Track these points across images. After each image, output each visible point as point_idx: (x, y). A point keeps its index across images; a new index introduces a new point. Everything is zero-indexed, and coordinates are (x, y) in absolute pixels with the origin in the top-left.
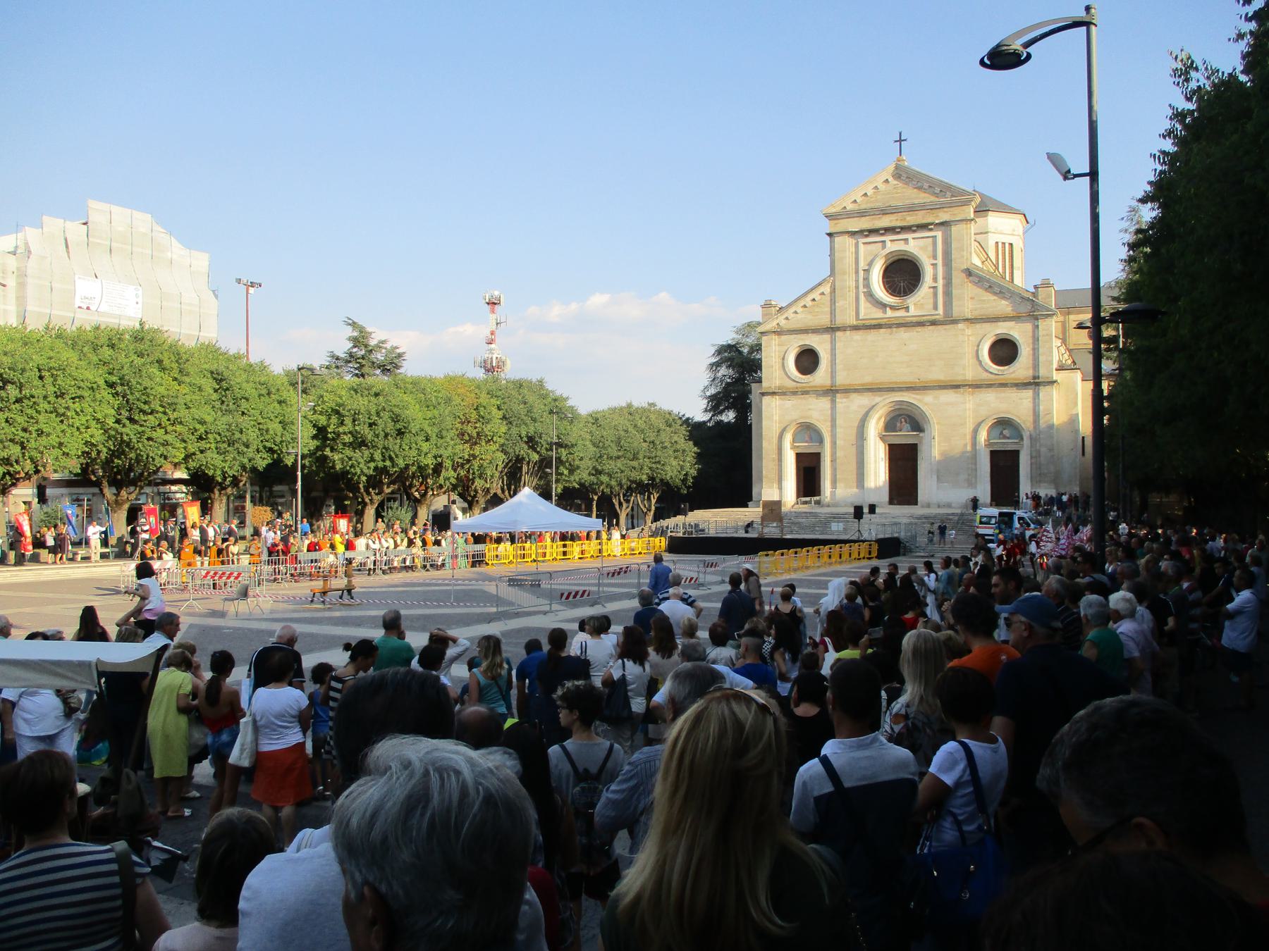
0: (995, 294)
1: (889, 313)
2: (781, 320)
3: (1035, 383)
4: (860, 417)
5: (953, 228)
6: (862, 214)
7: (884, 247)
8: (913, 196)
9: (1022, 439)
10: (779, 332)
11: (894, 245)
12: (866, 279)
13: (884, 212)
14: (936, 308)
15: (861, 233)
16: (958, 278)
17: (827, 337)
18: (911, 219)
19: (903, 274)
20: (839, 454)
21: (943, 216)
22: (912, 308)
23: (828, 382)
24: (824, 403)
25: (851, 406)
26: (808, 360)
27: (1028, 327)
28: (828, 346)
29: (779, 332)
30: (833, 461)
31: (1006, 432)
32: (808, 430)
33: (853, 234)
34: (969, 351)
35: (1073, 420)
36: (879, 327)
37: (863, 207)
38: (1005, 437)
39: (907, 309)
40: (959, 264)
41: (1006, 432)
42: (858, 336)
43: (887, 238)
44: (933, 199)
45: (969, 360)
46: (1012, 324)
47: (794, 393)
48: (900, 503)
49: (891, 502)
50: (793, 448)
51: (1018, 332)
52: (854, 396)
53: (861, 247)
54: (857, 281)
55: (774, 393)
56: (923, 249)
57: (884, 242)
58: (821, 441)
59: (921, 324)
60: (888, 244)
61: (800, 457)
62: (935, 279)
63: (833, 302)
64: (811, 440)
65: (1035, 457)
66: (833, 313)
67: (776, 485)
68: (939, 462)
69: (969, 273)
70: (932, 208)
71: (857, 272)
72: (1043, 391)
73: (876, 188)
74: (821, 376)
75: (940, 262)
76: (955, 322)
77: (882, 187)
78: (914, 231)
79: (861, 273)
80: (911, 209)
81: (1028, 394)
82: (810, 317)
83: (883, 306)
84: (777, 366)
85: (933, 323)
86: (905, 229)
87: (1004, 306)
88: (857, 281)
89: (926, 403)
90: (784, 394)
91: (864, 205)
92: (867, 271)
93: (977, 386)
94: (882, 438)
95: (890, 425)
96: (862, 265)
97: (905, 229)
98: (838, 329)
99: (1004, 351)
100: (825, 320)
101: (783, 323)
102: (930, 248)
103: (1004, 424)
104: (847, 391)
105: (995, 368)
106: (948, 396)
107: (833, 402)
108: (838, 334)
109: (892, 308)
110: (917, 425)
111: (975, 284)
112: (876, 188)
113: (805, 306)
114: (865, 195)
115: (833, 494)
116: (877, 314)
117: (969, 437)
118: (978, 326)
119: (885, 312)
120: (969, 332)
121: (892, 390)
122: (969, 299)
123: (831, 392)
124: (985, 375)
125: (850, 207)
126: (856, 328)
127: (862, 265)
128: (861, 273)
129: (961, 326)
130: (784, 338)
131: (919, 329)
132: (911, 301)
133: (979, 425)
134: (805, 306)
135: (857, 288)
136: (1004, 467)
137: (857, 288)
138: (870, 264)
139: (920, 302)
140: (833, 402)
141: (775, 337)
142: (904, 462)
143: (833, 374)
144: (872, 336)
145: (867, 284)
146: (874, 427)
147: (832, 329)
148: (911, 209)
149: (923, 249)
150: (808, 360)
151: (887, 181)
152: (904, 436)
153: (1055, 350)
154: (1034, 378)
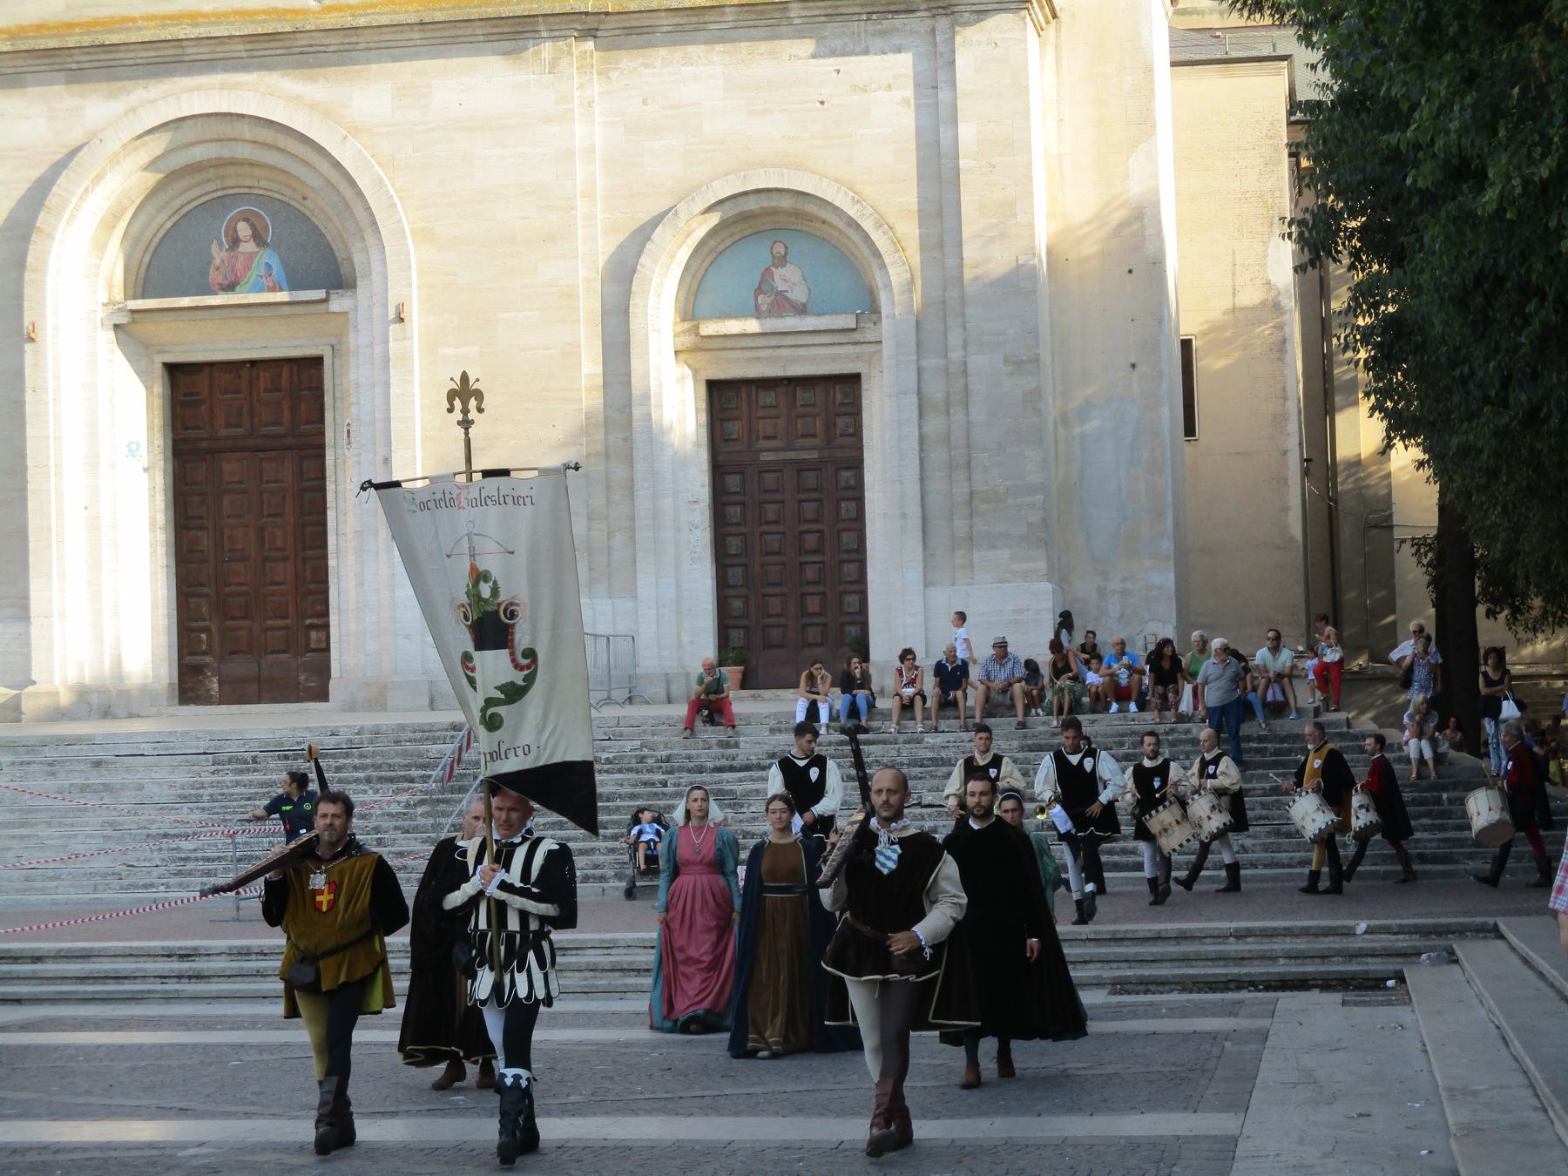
35: (1135, 253)
38: (783, 305)
41: (790, 280)
48: (237, 693)
49: (190, 684)
94: (127, 330)
95: (167, 261)
110: (324, 262)
117: (589, 304)
121: (167, 56)
133: (643, 235)
136: (784, 464)
142: (249, 457)
146: (80, 275)
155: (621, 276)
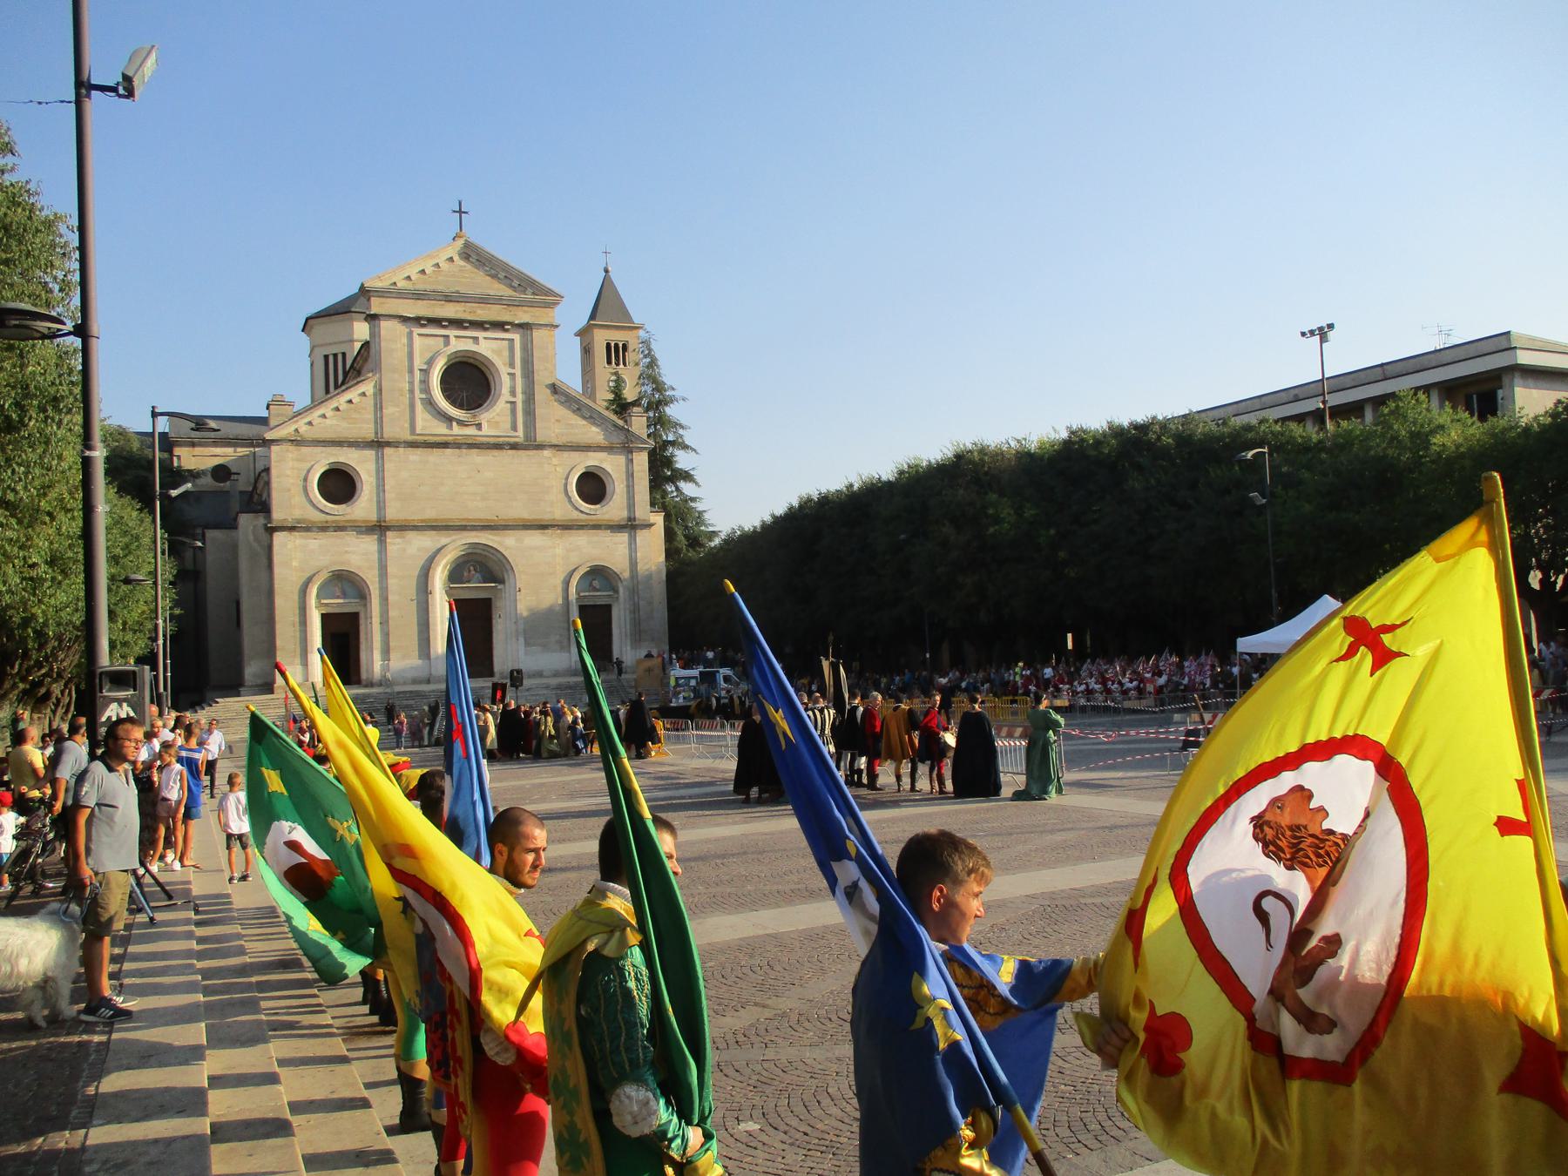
0: (584, 418)
1: (456, 430)
2: (301, 424)
3: (631, 526)
4: (421, 563)
5: (536, 333)
6: (418, 296)
7: (447, 343)
8: (481, 283)
9: (616, 591)
10: (297, 441)
11: (460, 343)
12: (425, 382)
13: (448, 298)
14: (514, 428)
15: (417, 321)
16: (542, 394)
17: (370, 454)
18: (483, 313)
19: (468, 382)
20: (392, 613)
21: (523, 316)
22: (485, 425)
23: (373, 517)
24: (369, 544)
25: (408, 550)
26: (339, 485)
27: (621, 459)
28: (372, 466)
29: (297, 441)
30: (385, 622)
31: (596, 583)
32: (344, 581)
33: (405, 320)
34: (557, 486)
36: (444, 445)
37: (421, 287)
38: (595, 590)
39: (479, 426)
40: (542, 378)
41: (596, 583)
42: (415, 455)
43: (452, 333)
44: (510, 292)
45: (556, 495)
46: (603, 455)
47: (323, 528)
50: (320, 605)
51: (612, 465)
52: (411, 535)
53: (416, 339)
54: (411, 383)
55: (292, 529)
56: (498, 352)
57: (447, 337)
58: (362, 595)
59: (498, 447)
60: (453, 340)
61: (326, 619)
62: (513, 393)
63: (379, 407)
64: (344, 595)
65: (635, 610)
66: (379, 422)
67: (298, 660)
68: (526, 620)
69: (554, 389)
70: (511, 304)
71: (411, 371)
72: (642, 536)
73: (437, 265)
74: (362, 507)
75: (518, 371)
76: (541, 447)
77: (444, 266)
78: (486, 329)
79: (417, 374)
80: (484, 300)
81: (624, 537)
82: (344, 424)
83: (450, 420)
84: (297, 490)
85: (514, 447)
86: (479, 325)
87: (595, 434)
88: (411, 383)
89: (506, 544)
90: (308, 529)
91: (421, 285)
92: (426, 372)
93: (567, 527)
95: (455, 575)
96: (419, 363)
97: (479, 325)
98: (388, 444)
99: (593, 487)
100: (368, 432)
101: (304, 429)
102: (506, 353)
103: (599, 574)
104: (403, 527)
106: (534, 539)
107: (382, 542)
108: (388, 451)
109: (461, 423)
111: (562, 403)
112: (437, 265)
113: (337, 409)
114: (423, 272)
115: (386, 668)
116: (440, 429)
117: (560, 589)
118: (566, 454)
119: (451, 428)
120: (555, 461)
121: (463, 528)
122: (555, 422)
123: (380, 528)
124: (575, 515)
125: (402, 284)
126: (413, 445)
127: (419, 363)
128: (417, 374)
129: (546, 453)
130: (305, 450)
131: (496, 452)
134: (337, 409)
135: (412, 391)
137: (412, 391)
138: (430, 362)
139: (495, 419)
140: (382, 542)
141: (292, 448)
142: (475, 620)
143: (381, 505)
144: (435, 456)
145: (426, 388)
147: (379, 444)
148: (484, 300)
149: (498, 352)
150: (339, 485)
151: (451, 259)
152: (474, 588)
154: (630, 519)
155: (567, 583)
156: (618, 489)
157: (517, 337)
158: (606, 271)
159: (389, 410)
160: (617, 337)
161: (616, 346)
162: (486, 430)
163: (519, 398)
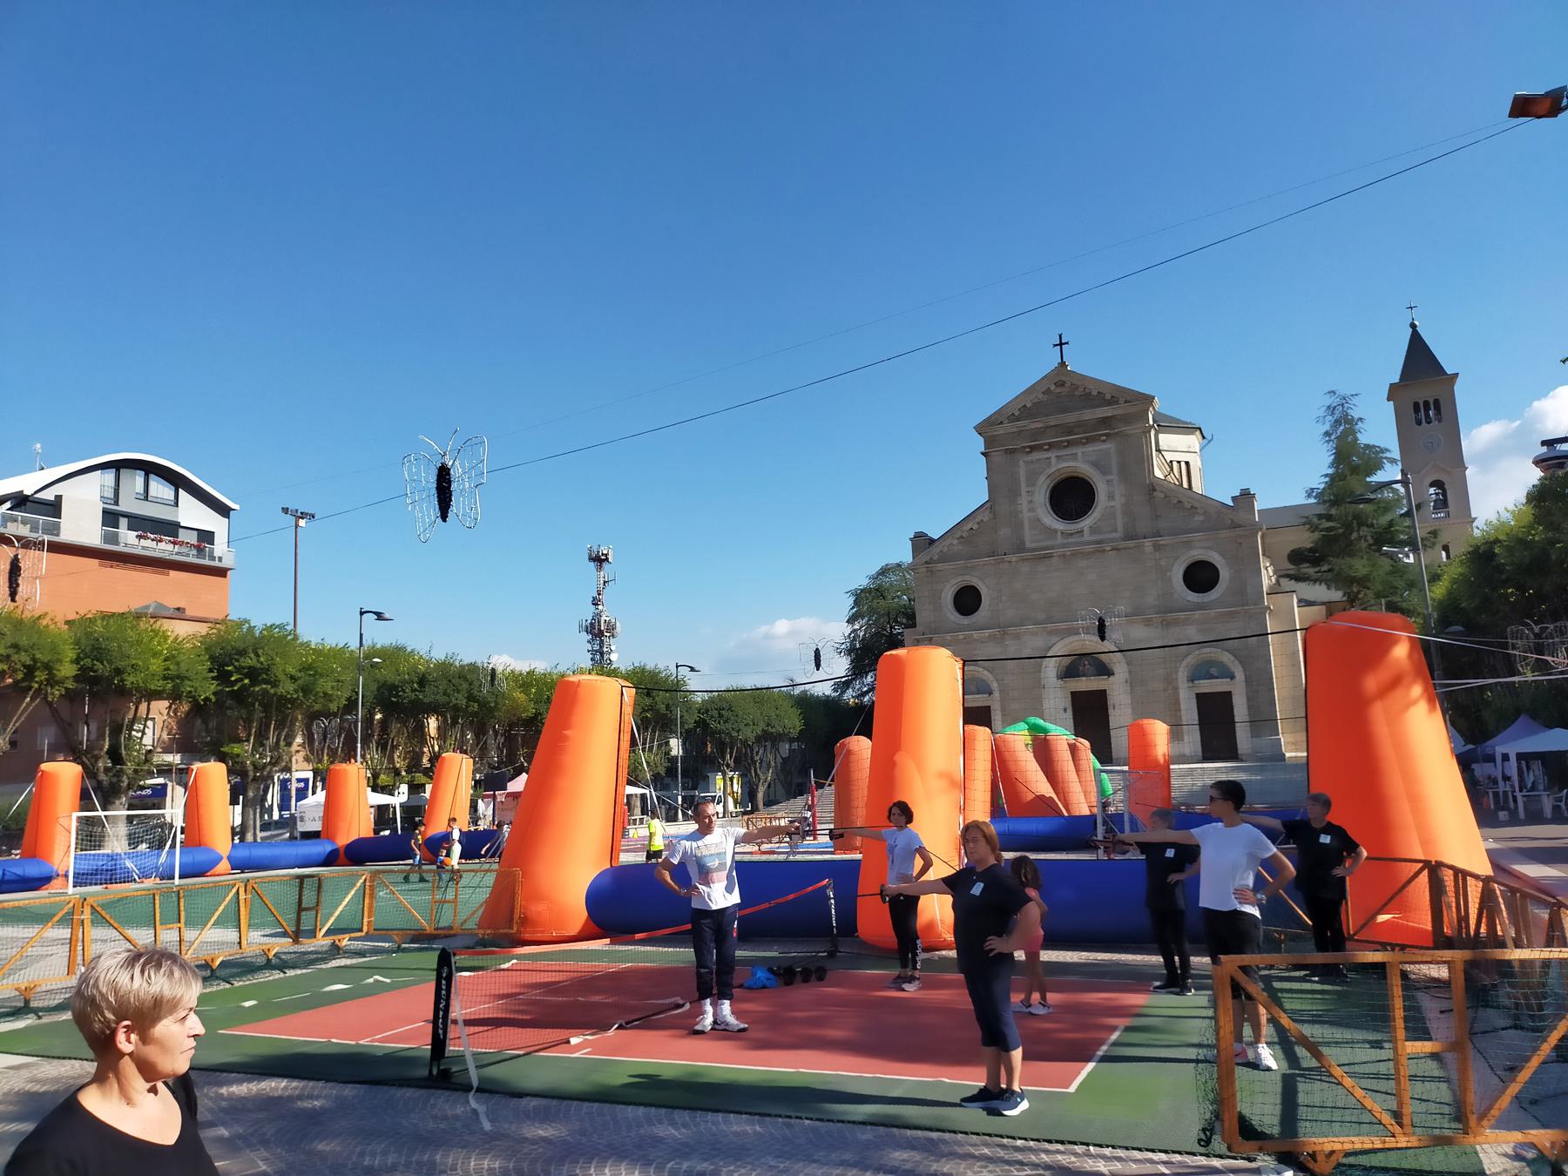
7: (1049, 465)
26: (967, 601)
43: (1052, 455)
56: (1096, 465)
60: (1054, 460)
75: (1114, 477)
83: (1056, 531)
105: (1193, 597)
132: (1086, 523)
150: (967, 601)
153: (1264, 572)
156: (1224, 574)
157: (1109, 446)
158: (1413, 326)
159: (1004, 532)
160: (1423, 393)
161: (1426, 404)
162: (1087, 537)
163: (1118, 502)
